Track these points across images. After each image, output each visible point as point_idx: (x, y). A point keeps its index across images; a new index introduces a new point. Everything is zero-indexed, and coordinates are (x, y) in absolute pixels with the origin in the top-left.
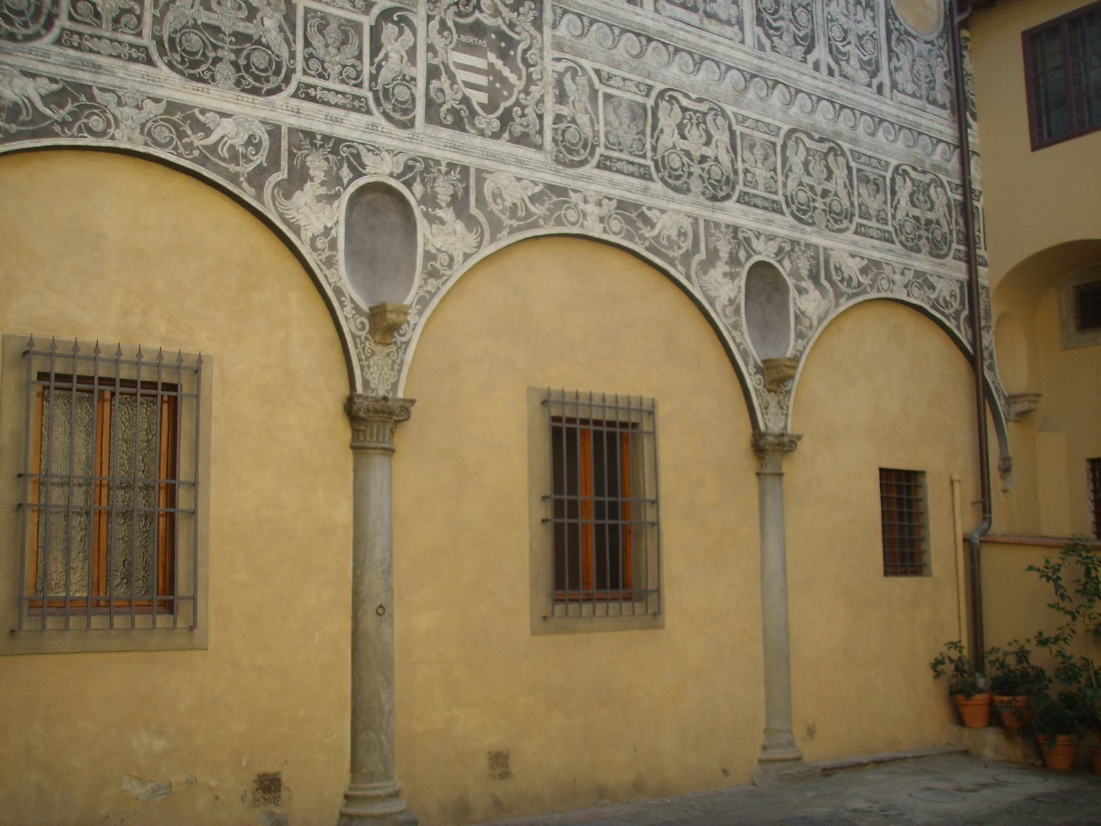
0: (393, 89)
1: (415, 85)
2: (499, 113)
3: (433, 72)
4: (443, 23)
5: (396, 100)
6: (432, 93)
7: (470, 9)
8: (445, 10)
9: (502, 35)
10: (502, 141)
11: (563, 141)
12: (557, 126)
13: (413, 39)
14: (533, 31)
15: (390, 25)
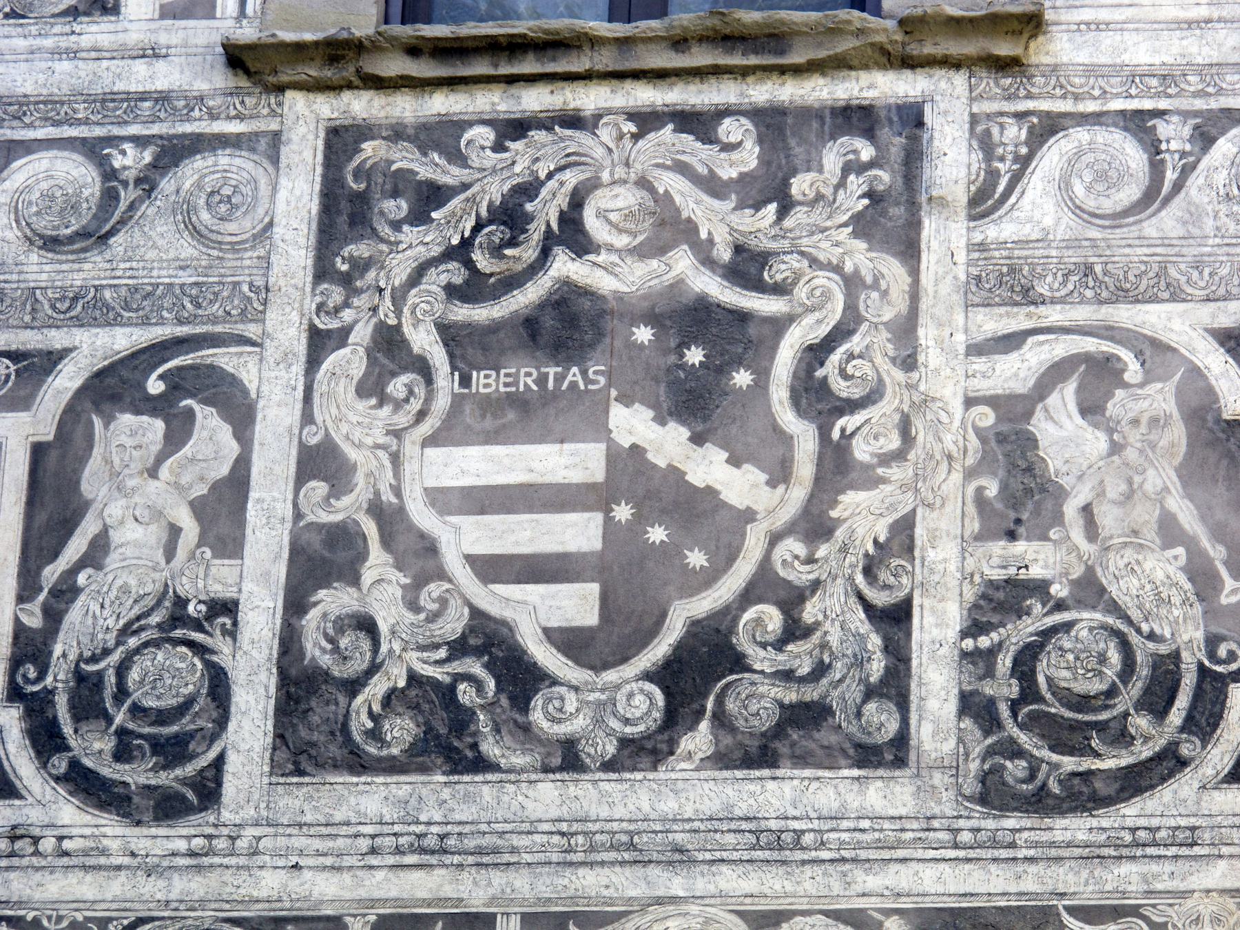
0: (122, 670)
1: (232, 633)
2: (659, 650)
3: (321, 560)
4: (389, 346)
5: (137, 711)
6: (315, 648)
7: (528, 253)
8: (398, 299)
9: (693, 318)
10: (678, 769)
11: (1030, 693)
12: (984, 642)
13: (233, 448)
14: (860, 256)
15: (127, 419)
